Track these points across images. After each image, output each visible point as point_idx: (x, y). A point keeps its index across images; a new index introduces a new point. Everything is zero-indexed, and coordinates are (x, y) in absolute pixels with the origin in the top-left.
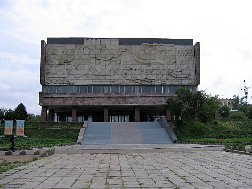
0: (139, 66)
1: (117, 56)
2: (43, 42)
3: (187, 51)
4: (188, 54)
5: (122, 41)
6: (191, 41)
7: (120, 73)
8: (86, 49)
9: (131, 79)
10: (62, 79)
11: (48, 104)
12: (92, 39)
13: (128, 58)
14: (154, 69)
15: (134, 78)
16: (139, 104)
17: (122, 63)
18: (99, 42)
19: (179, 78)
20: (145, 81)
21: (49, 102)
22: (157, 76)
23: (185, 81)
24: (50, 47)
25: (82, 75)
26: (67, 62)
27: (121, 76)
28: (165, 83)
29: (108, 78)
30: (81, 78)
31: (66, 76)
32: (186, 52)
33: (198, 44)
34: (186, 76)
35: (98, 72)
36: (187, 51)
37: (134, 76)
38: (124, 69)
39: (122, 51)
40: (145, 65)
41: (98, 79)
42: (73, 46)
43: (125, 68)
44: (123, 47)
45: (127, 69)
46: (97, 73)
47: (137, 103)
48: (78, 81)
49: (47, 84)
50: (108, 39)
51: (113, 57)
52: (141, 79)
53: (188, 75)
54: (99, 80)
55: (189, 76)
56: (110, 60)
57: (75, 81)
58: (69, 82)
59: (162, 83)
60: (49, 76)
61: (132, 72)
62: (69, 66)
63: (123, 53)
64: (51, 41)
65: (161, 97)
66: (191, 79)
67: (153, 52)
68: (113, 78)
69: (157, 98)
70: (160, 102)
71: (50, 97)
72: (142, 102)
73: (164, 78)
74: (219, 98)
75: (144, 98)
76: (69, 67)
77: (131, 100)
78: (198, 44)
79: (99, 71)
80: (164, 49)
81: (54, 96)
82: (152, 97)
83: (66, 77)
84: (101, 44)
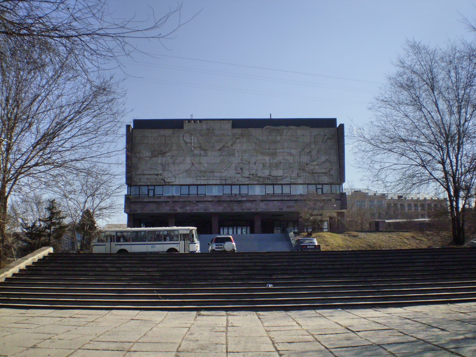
0: (260, 157)
1: (229, 144)
2: (128, 127)
3: (327, 136)
4: (329, 141)
5: (237, 124)
6: (334, 120)
7: (234, 168)
8: (188, 135)
9: (248, 176)
10: (156, 177)
11: (136, 210)
12: (195, 121)
13: (245, 147)
14: (280, 163)
15: (253, 175)
16: (260, 210)
17: (237, 155)
18: (204, 126)
19: (316, 175)
20: (268, 178)
21: (139, 210)
22: (285, 170)
23: (324, 177)
24: (139, 133)
25: (182, 172)
26: (161, 154)
27: (235, 172)
28: (296, 180)
29: (218, 174)
30: (181, 176)
31: (160, 172)
32: (326, 138)
33: (342, 126)
34: (325, 172)
35: (204, 167)
36: (327, 136)
37: (253, 172)
38: (239, 163)
39: (237, 138)
40: (268, 157)
41: (204, 177)
42: (168, 132)
43: (240, 161)
44: (238, 131)
45: (243, 162)
46: (203, 169)
47: (256, 209)
48: (177, 179)
49: (135, 184)
50: (217, 121)
51: (223, 146)
52: (263, 175)
53: (328, 170)
54: (206, 178)
55: (329, 171)
56: (220, 150)
57: (173, 180)
58: (164, 181)
59: (292, 181)
60: (137, 173)
61: (250, 166)
62: (164, 159)
63: (238, 141)
64: (140, 124)
65: (289, 200)
66: (332, 175)
67: (279, 138)
68: (224, 175)
69: (285, 202)
70: (288, 207)
71: (140, 202)
72: (264, 207)
73: (294, 175)
74: (412, 198)
75: (267, 202)
76: (164, 161)
77: (249, 205)
78: (342, 126)
79: (206, 165)
80: (295, 134)
81: (144, 201)
82: (278, 200)
83: (161, 174)
84: (207, 128)
